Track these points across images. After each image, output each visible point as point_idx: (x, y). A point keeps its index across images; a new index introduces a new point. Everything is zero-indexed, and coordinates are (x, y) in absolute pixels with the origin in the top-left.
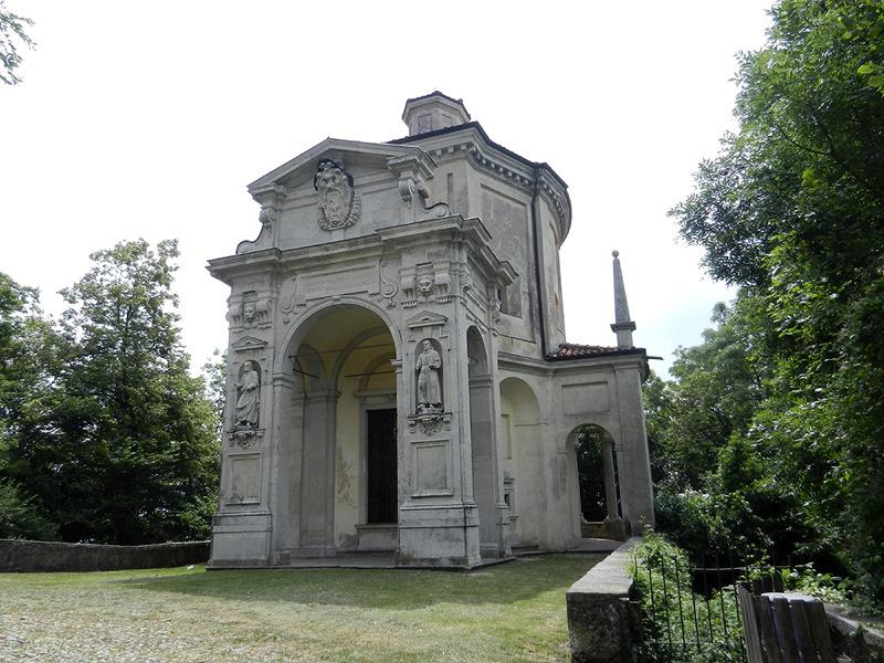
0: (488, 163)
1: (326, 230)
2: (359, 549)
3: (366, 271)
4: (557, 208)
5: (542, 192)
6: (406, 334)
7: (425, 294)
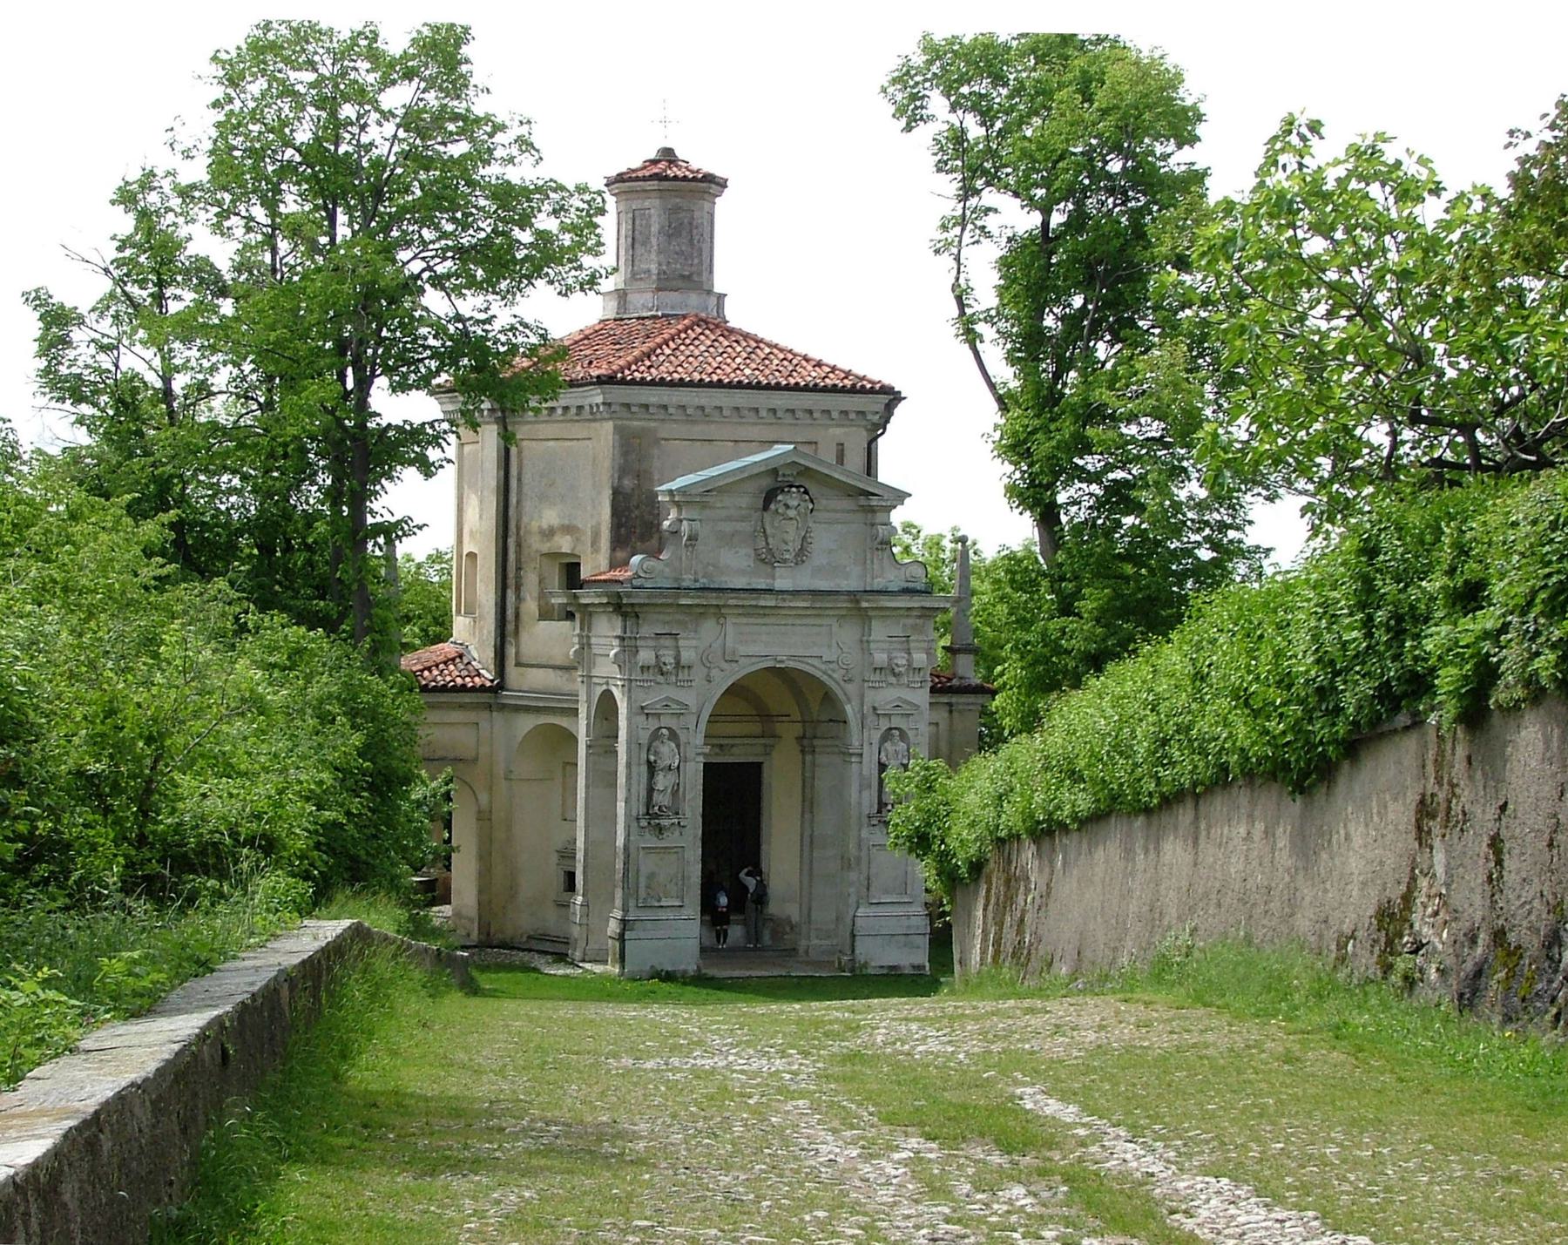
6: (871, 718)
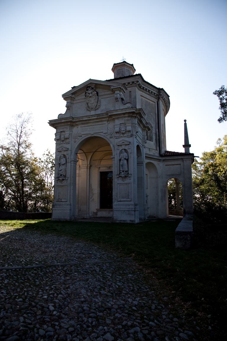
0: (143, 88)
1: (89, 111)
2: (97, 216)
3: (102, 125)
4: (165, 104)
5: (161, 98)
6: (116, 147)
7: (123, 134)
